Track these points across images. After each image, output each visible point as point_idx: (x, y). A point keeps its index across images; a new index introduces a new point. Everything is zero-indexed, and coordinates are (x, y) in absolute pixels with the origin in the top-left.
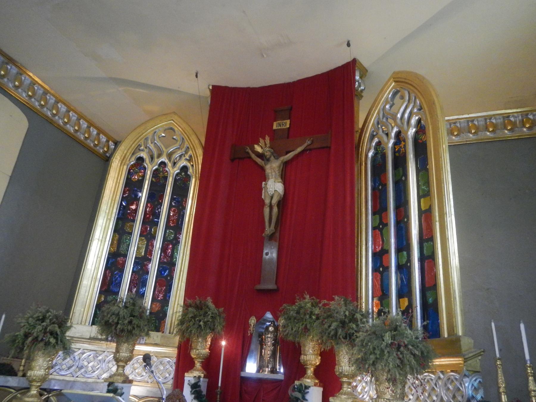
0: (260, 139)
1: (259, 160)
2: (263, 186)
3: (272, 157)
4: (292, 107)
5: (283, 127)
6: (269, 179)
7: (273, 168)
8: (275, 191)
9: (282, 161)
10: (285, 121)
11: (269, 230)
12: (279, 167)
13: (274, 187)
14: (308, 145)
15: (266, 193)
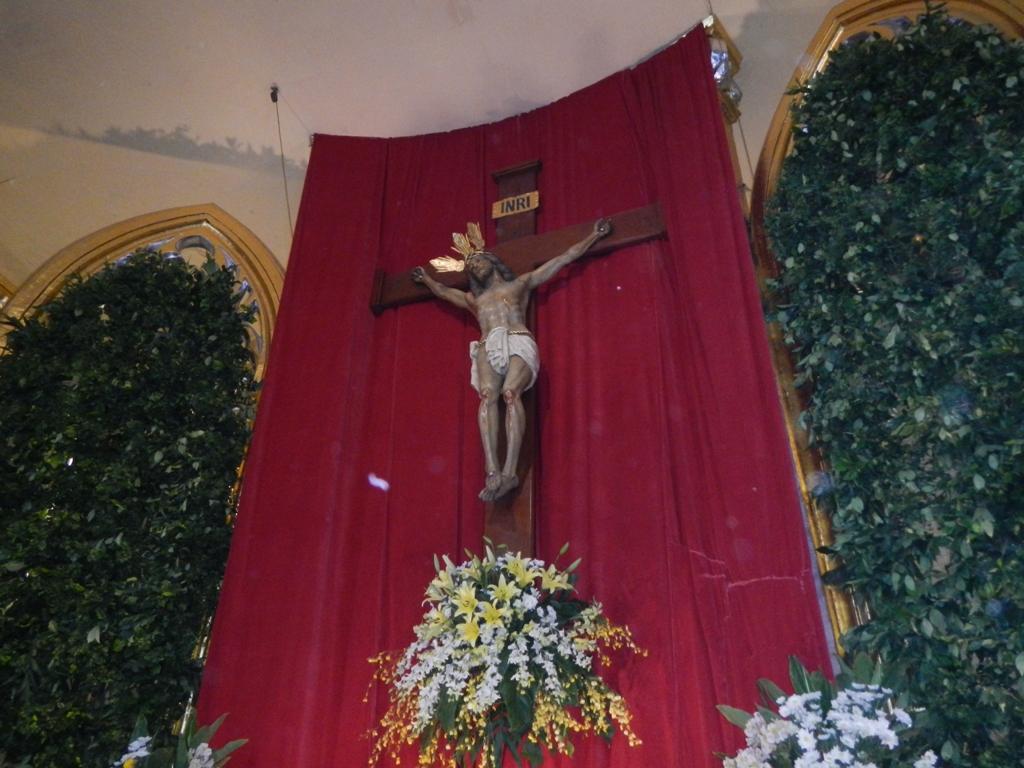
0: (454, 234)
1: (456, 296)
2: (473, 351)
3: (496, 276)
4: (540, 165)
5: (522, 210)
6: (489, 330)
7: (496, 305)
8: (511, 357)
9: (526, 284)
10: (525, 196)
11: (499, 476)
12: (520, 296)
13: (505, 348)
14: (602, 238)
15: (485, 367)
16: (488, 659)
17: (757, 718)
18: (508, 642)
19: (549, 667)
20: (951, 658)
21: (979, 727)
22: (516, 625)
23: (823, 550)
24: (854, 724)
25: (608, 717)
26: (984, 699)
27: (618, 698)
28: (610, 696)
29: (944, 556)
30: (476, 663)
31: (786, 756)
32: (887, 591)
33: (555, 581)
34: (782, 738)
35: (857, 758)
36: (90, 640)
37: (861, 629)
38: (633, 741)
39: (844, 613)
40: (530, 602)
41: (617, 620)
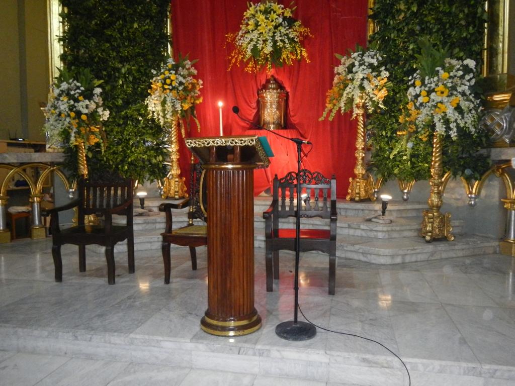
16: (268, 38)
17: (345, 57)
18: (274, 33)
19: (286, 41)
20: (396, 44)
21: (397, 60)
22: (276, 27)
23: (371, 9)
24: (368, 60)
25: (301, 55)
26: (400, 54)
27: (305, 50)
28: (302, 49)
29: (403, 15)
30: (264, 39)
31: (351, 67)
32: (385, 22)
33: (288, 14)
34: (351, 63)
35: (367, 68)
36: (135, 27)
37: (376, 33)
38: (308, 61)
39: (372, 28)
40: (280, 20)
41: (306, 27)
